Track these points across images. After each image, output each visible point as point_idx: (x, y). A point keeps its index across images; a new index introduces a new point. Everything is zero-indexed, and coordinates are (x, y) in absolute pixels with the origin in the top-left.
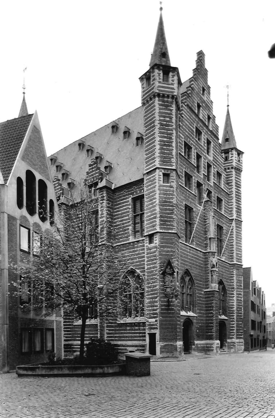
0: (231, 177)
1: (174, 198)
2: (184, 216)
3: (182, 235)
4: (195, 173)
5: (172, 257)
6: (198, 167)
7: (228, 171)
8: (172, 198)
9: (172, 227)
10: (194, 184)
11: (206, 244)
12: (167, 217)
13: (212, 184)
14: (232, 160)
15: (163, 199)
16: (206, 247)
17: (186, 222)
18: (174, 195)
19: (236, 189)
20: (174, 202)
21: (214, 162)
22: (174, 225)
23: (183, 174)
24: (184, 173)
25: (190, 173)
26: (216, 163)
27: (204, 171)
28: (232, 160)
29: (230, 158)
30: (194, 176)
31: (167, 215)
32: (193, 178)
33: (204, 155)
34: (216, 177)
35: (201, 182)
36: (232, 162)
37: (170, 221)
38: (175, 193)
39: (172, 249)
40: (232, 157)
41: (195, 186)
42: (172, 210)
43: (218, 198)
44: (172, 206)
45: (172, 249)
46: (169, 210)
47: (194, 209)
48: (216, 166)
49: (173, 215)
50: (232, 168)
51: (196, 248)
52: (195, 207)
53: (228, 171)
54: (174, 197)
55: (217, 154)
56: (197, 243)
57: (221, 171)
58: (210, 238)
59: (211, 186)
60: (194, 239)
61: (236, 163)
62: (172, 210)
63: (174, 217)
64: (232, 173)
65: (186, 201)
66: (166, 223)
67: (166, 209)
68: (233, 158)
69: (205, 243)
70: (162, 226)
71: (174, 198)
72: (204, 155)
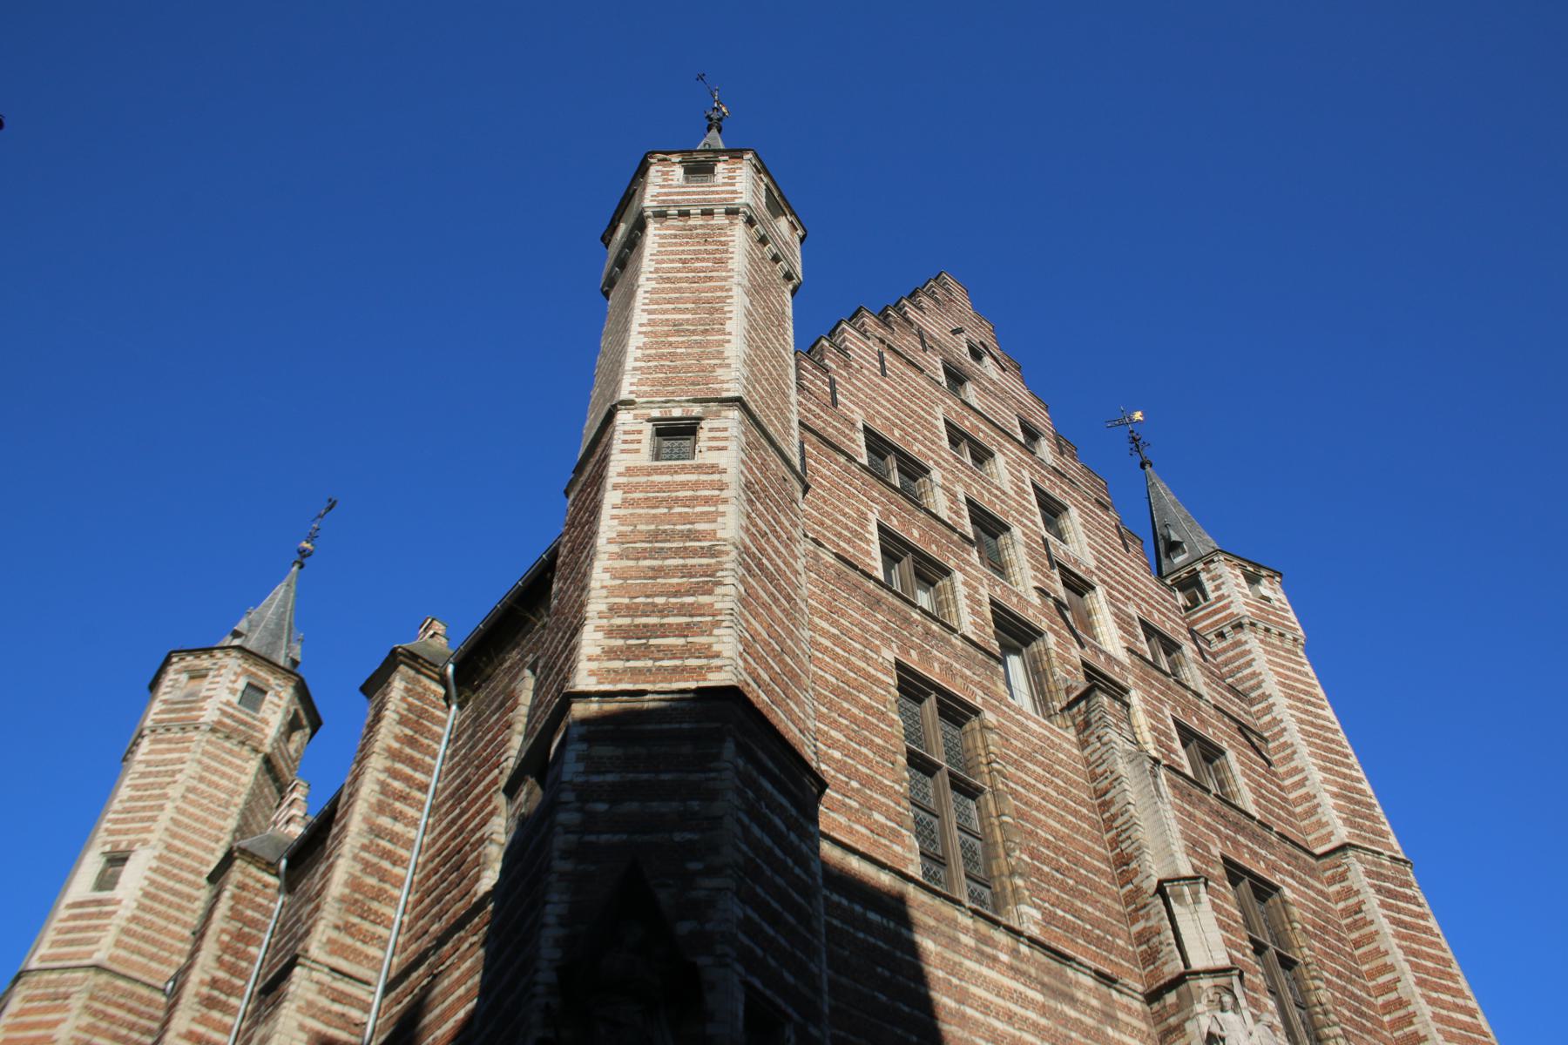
0: (1249, 664)
1: (723, 514)
2: (896, 717)
3: (876, 816)
4: (971, 565)
5: (694, 866)
6: (999, 567)
7: (1224, 644)
8: (711, 518)
9: (703, 662)
10: (963, 603)
11: (1142, 938)
12: (662, 611)
13: (1122, 656)
14: (1220, 598)
15: (639, 527)
16: (1151, 957)
17: (920, 764)
18: (725, 501)
19: (1290, 707)
20: (720, 534)
21: (1109, 576)
22: (716, 648)
23: (863, 526)
24: (873, 528)
25: (932, 551)
26: (1118, 583)
27: (1035, 578)
28: (1220, 598)
29: (1212, 596)
30: (961, 570)
31: (660, 600)
32: (958, 577)
33: (1025, 526)
34: (1143, 638)
35: (1034, 611)
36: (1225, 607)
37: (682, 631)
38: (725, 494)
39: (695, 805)
40: (1218, 588)
41: (974, 612)
42: (710, 572)
43: (1187, 735)
44: (711, 552)
45: (695, 805)
46: (687, 572)
47: (990, 717)
48: (1128, 598)
49: (710, 592)
50: (1239, 626)
51: (1053, 944)
52: (993, 709)
53: (1224, 644)
54: (721, 508)
55: (1121, 560)
56: (1049, 918)
57: (1171, 626)
58: (1160, 890)
59: (1109, 657)
60: (1019, 882)
61: (1247, 604)
62: (710, 572)
63: (718, 606)
64: (1247, 647)
65: (904, 649)
66: (652, 642)
67: (658, 572)
68: (1224, 590)
69: (1140, 934)
70: (618, 664)
71: (723, 514)
72: (1020, 522)
